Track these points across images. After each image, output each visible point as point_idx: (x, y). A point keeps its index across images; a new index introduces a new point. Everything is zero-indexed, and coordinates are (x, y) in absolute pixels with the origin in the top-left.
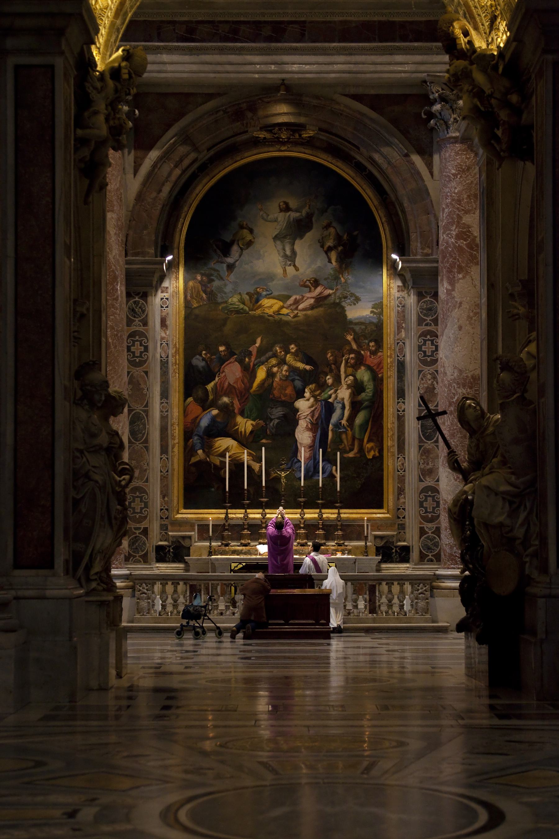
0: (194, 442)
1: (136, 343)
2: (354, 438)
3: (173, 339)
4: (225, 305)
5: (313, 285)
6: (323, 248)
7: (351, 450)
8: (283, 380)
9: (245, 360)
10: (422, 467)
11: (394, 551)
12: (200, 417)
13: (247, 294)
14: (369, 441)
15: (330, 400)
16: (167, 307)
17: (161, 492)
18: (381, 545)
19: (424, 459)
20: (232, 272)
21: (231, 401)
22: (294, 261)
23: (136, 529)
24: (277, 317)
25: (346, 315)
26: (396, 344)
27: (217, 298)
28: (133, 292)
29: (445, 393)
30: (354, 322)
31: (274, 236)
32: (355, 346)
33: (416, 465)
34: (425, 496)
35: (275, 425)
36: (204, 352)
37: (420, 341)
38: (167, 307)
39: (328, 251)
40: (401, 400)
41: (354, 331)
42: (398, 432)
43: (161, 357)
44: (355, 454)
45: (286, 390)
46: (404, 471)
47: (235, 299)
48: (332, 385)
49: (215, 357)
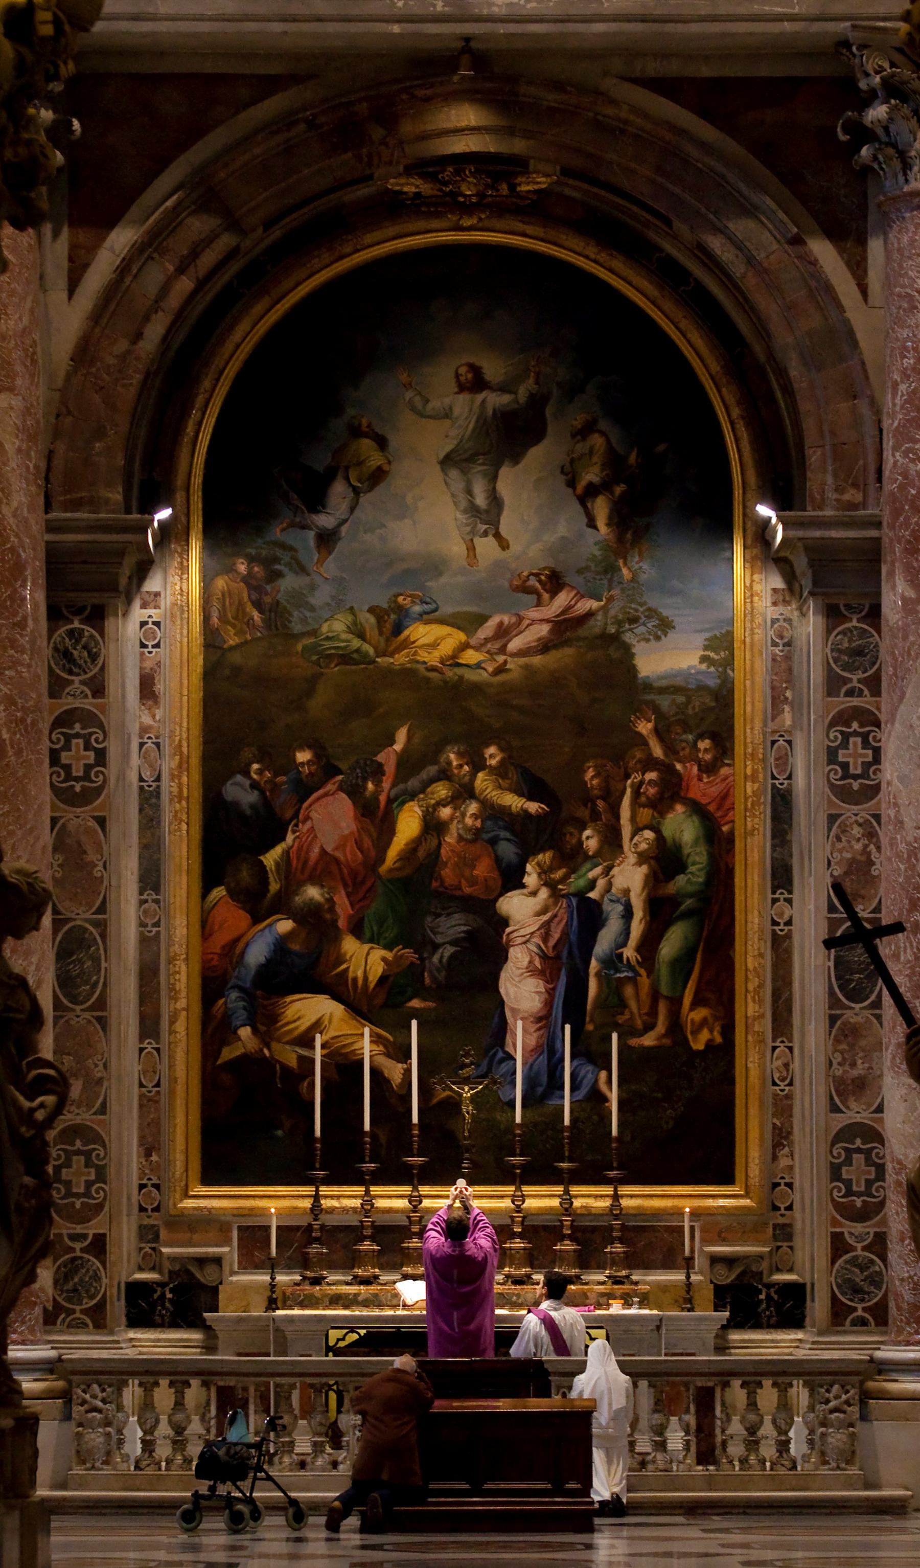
0: (230, 1006)
1: (74, 741)
2: (655, 995)
3: (172, 732)
4: (312, 640)
5: (548, 586)
6: (574, 489)
7: (649, 1027)
8: (466, 840)
9: (365, 788)
10: (839, 1073)
11: (762, 1297)
13: (371, 610)
14: (694, 1005)
15: (592, 895)
16: (157, 646)
17: (142, 1139)
18: (729, 1281)
19: (842, 1053)
20: (330, 553)
21: (327, 896)
22: (495, 524)
23: (74, 1237)
24: (450, 673)
25: (634, 667)
26: (769, 744)
27: (290, 622)
28: (67, 607)
29: (899, 875)
30: (656, 685)
31: (442, 455)
32: (658, 751)
33: (823, 1067)
34: (846, 1149)
35: (444, 960)
36: (255, 766)
37: (832, 736)
38: (157, 646)
39: (586, 497)
40: (782, 893)
41: (656, 710)
42: (774, 980)
43: (141, 779)
44: (659, 1038)
45: (473, 867)
46: (791, 1084)
47: (338, 626)
48: (598, 853)
49: (284, 778)
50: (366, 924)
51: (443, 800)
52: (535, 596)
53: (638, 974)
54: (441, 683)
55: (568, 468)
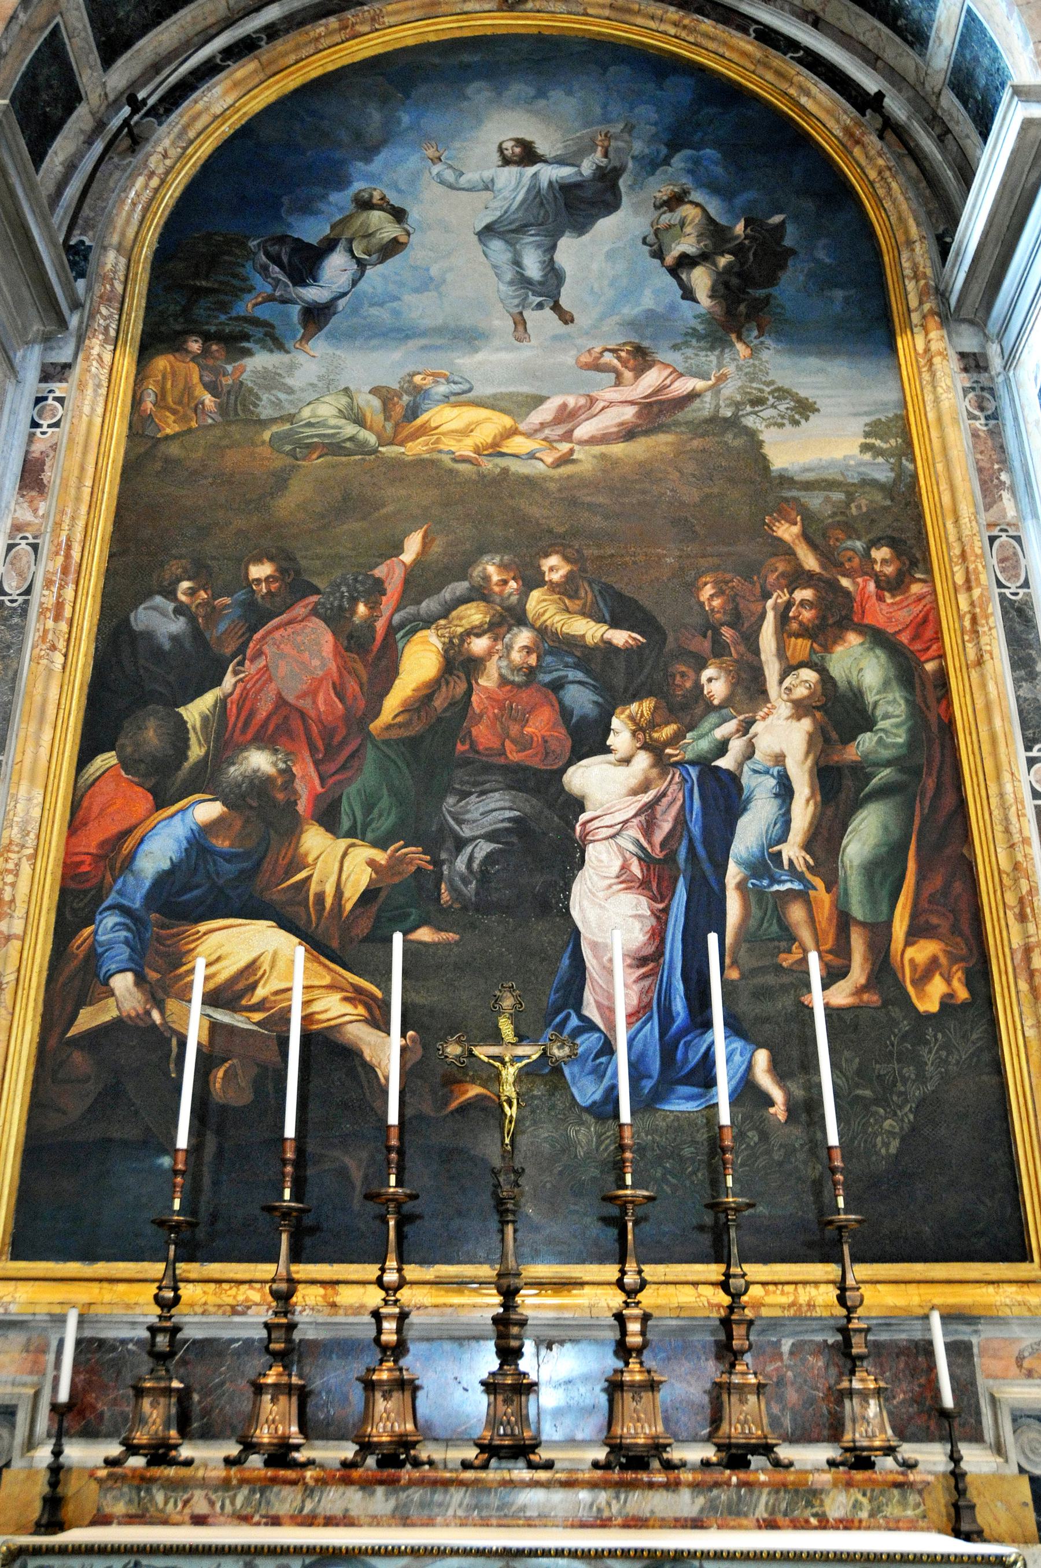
8: (512, 683)
9: (353, 611)
12: (137, 834)
13: (375, 391)
20: (320, 329)
21: (282, 766)
24: (489, 465)
25: (764, 458)
27: (256, 406)
32: (810, 562)
36: (185, 585)
48: (728, 702)
49: (227, 600)
50: (345, 806)
51: (473, 628)
52: (613, 376)
54: (474, 477)
55: (651, 239)
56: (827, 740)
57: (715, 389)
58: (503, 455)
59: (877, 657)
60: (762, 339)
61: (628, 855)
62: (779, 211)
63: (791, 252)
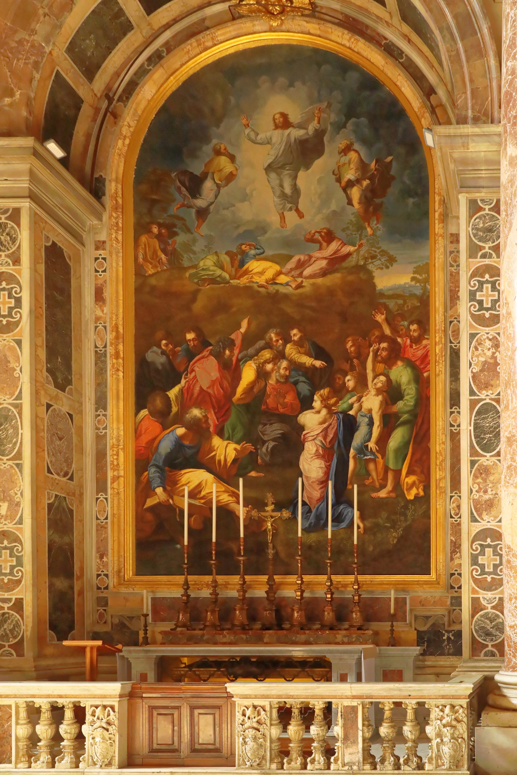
0: (151, 476)
2: (386, 469)
4: (194, 271)
5: (326, 239)
6: (340, 183)
7: (383, 486)
9: (224, 353)
13: (227, 253)
20: (204, 221)
21: (204, 414)
22: (296, 203)
24: (272, 289)
27: (182, 260)
30: (386, 294)
31: (266, 165)
32: (387, 331)
34: (481, 545)
35: (269, 450)
36: (164, 342)
41: (386, 307)
45: (285, 397)
48: (354, 389)
49: (179, 349)
50: (226, 429)
51: (267, 360)
52: (318, 245)
53: (376, 457)
55: (336, 172)
56: (387, 404)
57: (357, 251)
58: (277, 284)
59: (408, 371)
60: (378, 225)
61: (318, 446)
62: (391, 155)
63: (393, 178)
